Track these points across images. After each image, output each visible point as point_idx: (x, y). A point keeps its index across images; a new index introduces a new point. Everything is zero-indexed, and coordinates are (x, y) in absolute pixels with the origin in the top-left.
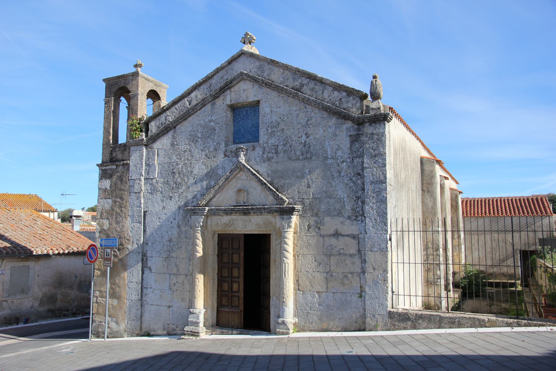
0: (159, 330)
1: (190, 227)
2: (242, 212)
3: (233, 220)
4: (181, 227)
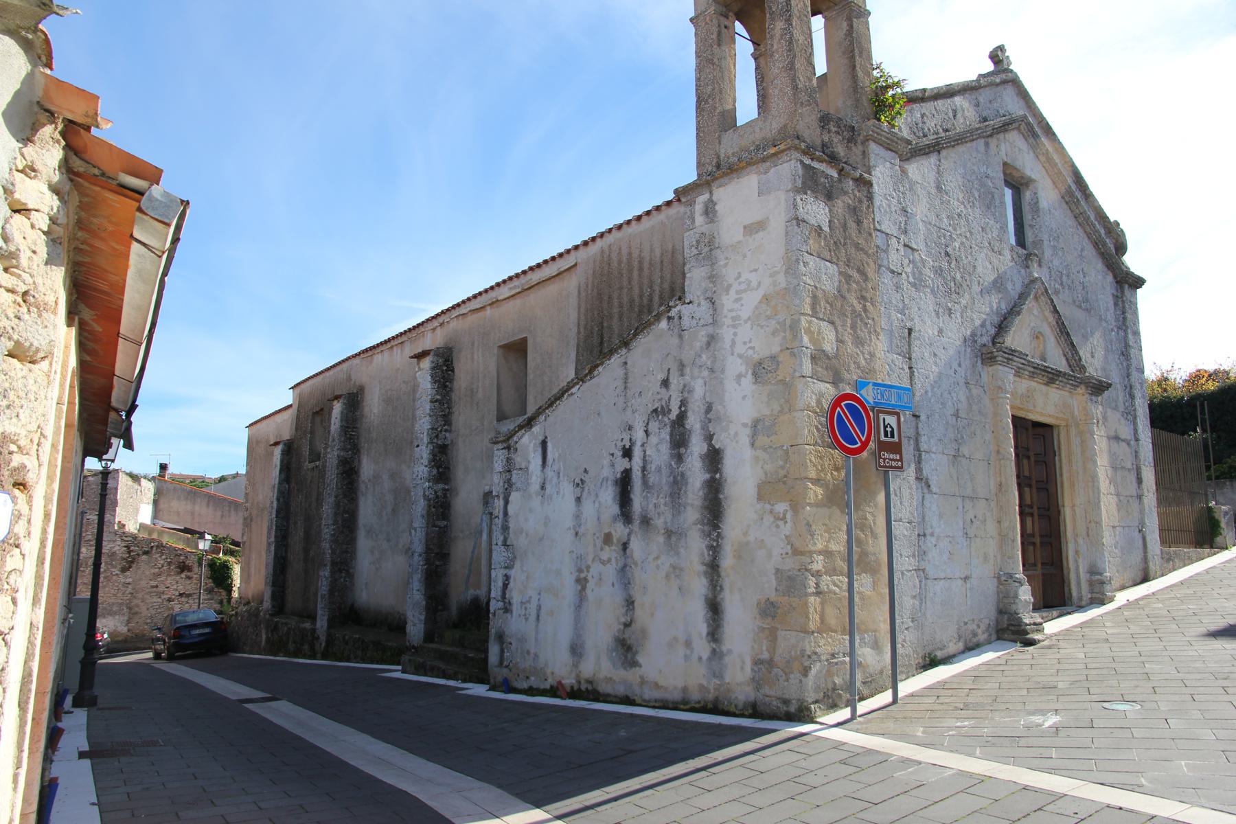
0: (951, 644)
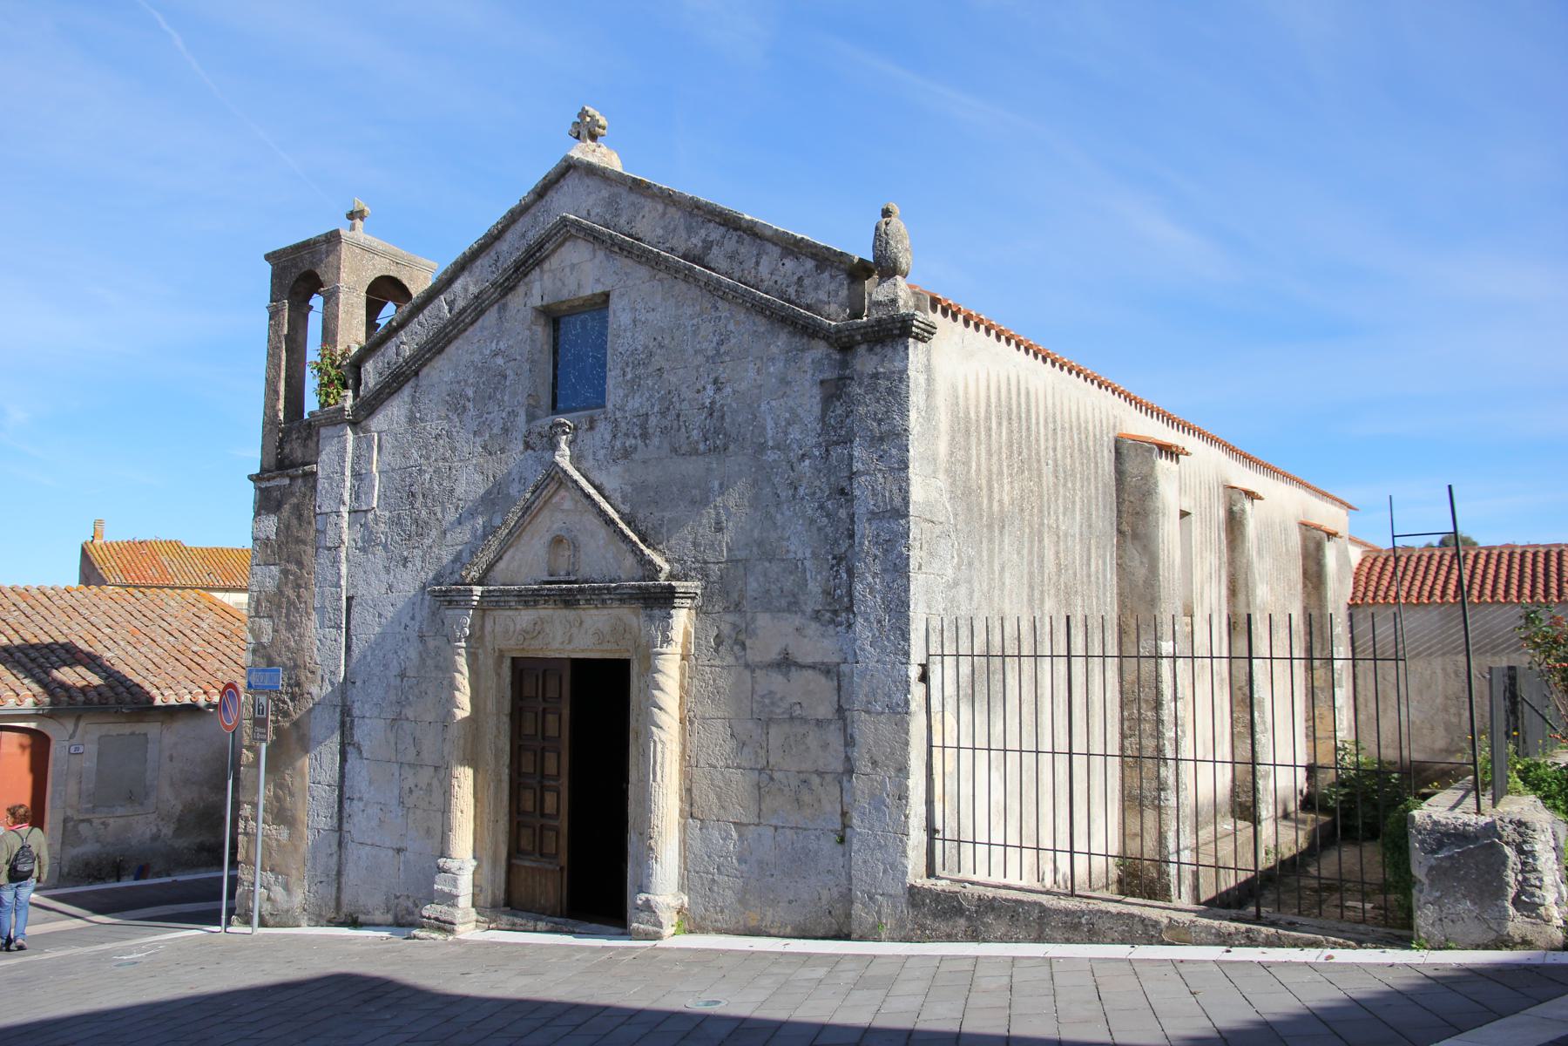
0: (377, 913)
2: (557, 598)
3: (541, 619)
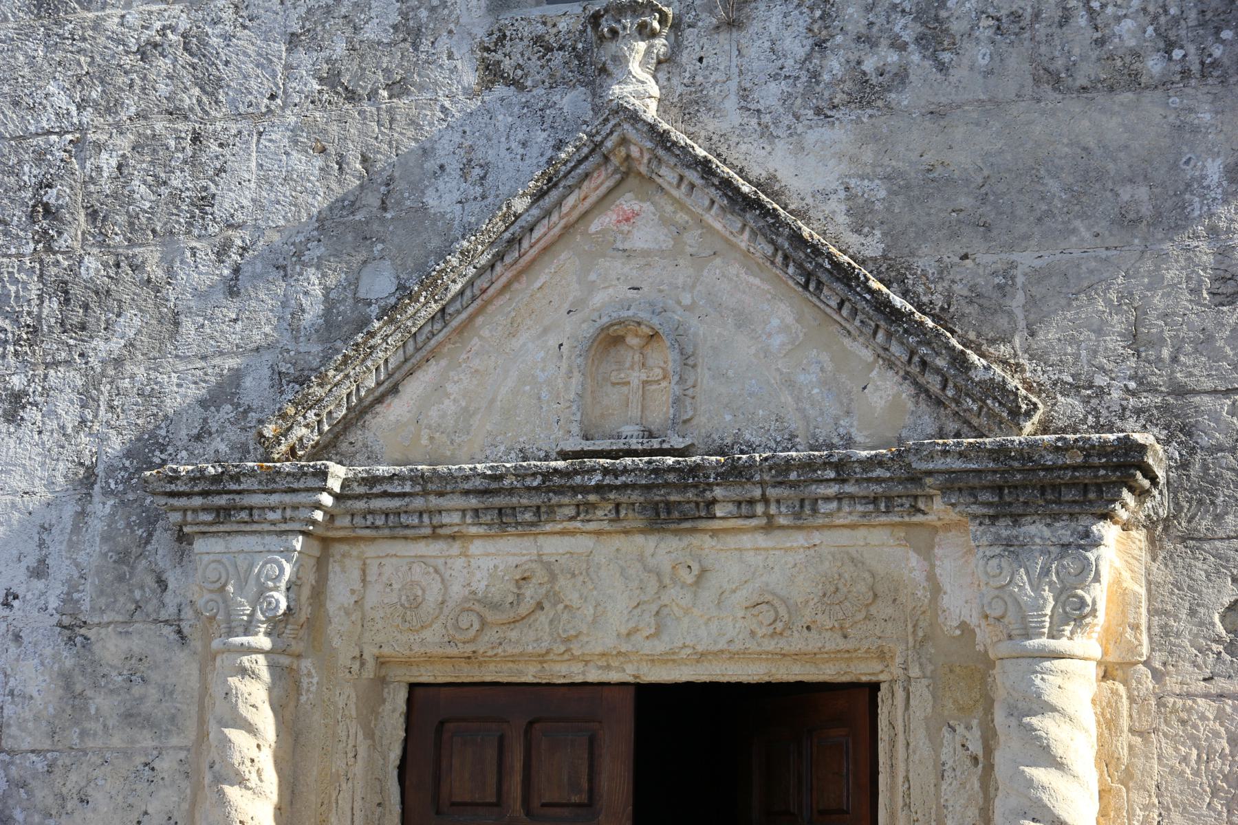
1: (168, 631)
2: (636, 497)
3: (548, 566)
4: (91, 634)
